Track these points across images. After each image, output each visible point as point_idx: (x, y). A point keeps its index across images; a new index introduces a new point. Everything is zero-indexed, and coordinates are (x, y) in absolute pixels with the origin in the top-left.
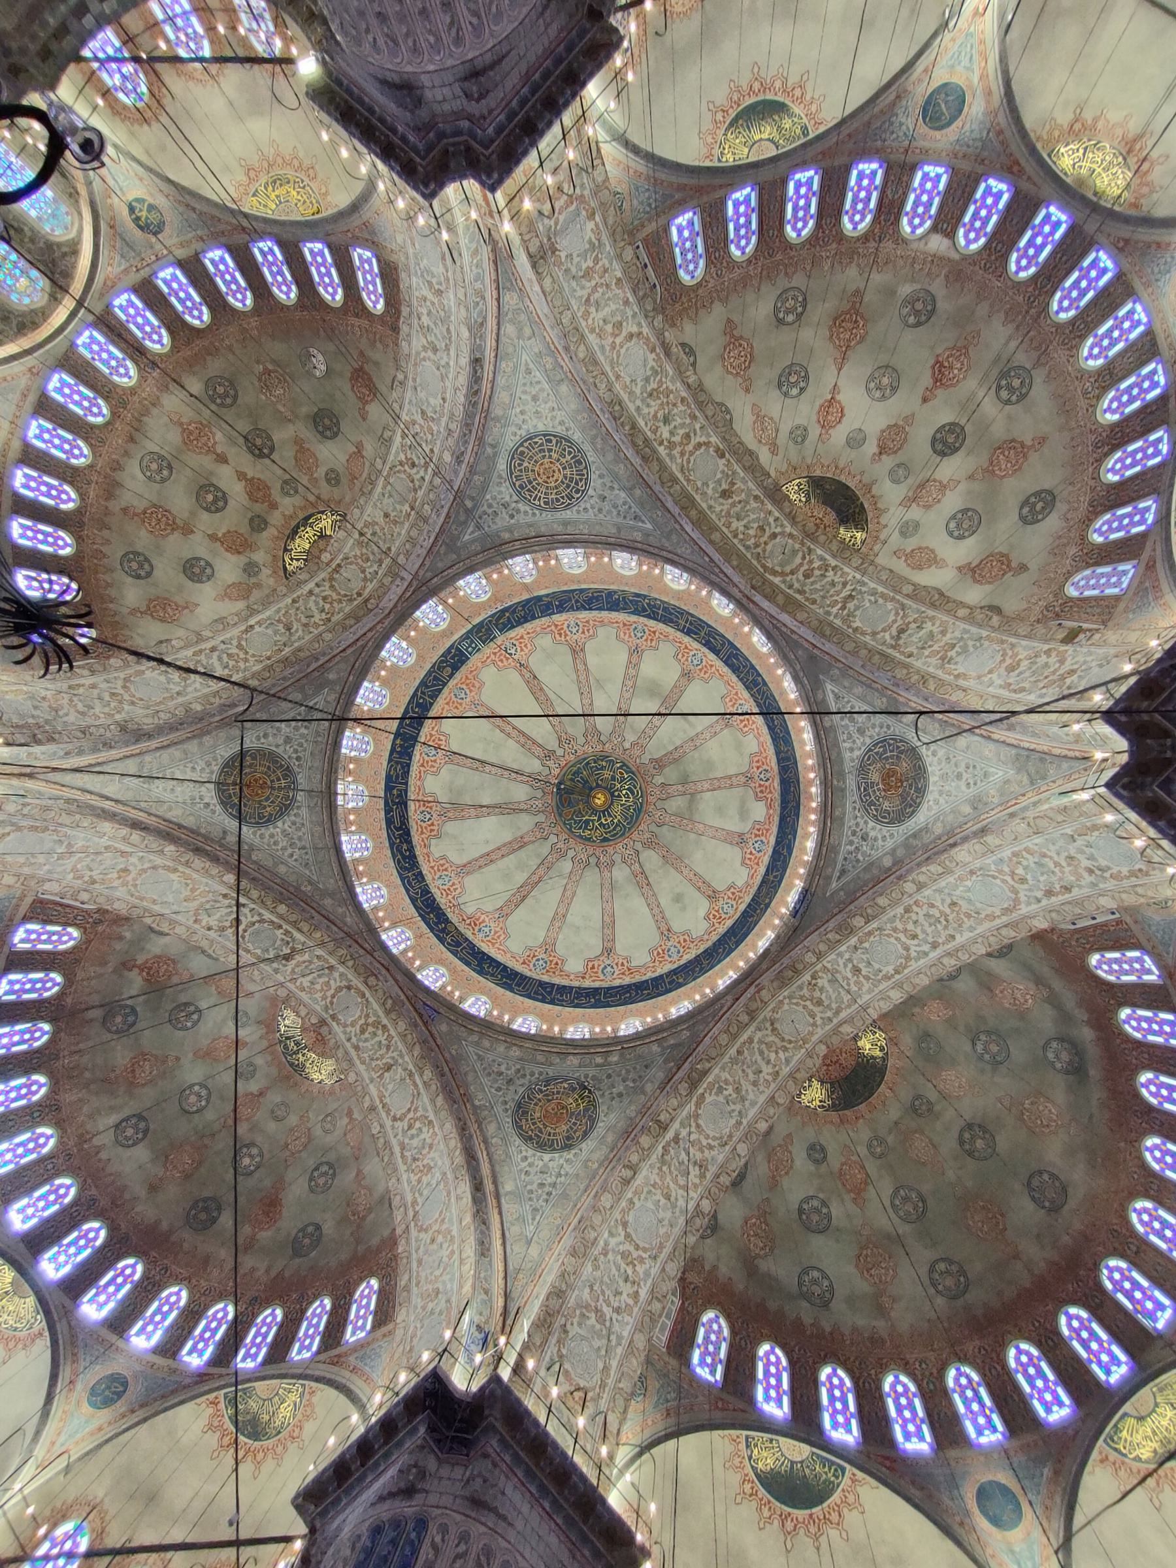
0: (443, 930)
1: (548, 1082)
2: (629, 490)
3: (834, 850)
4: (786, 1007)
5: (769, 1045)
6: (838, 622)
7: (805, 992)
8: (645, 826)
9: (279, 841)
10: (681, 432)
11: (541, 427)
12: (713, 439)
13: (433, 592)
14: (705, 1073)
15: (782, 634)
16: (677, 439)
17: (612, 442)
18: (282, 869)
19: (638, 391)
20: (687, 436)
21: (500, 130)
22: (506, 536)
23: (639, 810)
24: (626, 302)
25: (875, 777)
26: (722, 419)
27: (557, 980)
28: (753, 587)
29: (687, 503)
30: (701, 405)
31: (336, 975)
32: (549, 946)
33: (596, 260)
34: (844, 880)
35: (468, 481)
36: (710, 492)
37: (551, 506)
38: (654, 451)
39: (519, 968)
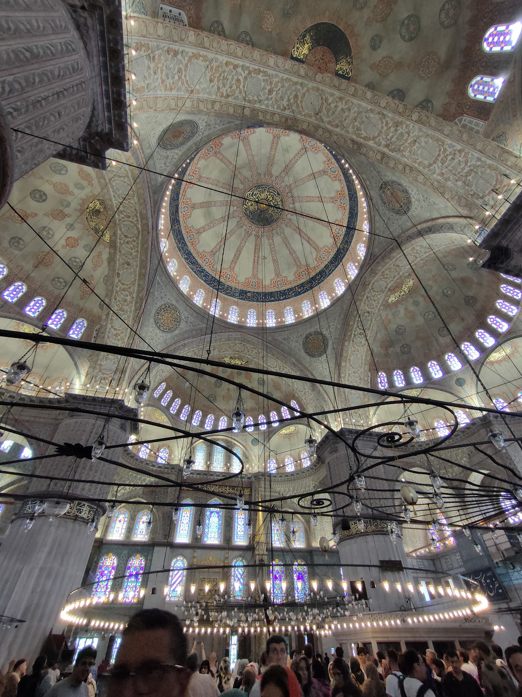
0: (343, 250)
1: (385, 203)
3: (223, 130)
4: (306, 111)
5: (328, 111)
6: (136, 198)
7: (294, 107)
8: (264, 180)
9: (330, 330)
11: (158, 331)
12: (117, 280)
13: (227, 323)
14: (353, 141)
15: (155, 208)
18: (339, 327)
20: (123, 290)
22: (195, 314)
23: (258, 187)
24: (108, 337)
25: (181, 139)
27: (346, 192)
28: (148, 233)
29: (142, 276)
30: (112, 292)
31: (369, 295)
32: (333, 200)
34: (232, 121)
35: (188, 338)
36: (132, 270)
37: (175, 309)
38: (137, 297)
39: (347, 211)
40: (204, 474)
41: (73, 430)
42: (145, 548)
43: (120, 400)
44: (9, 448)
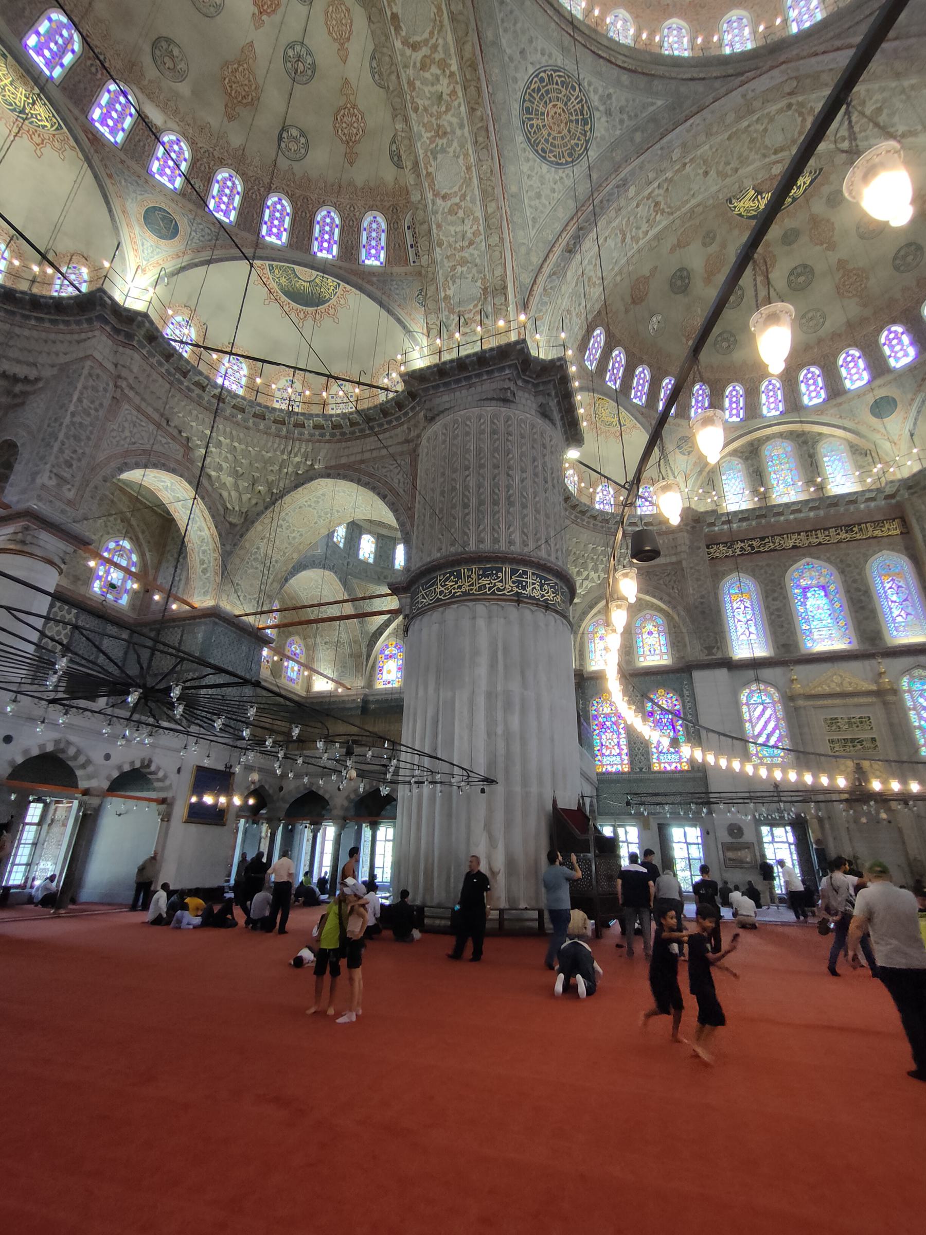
2: (495, 43)
10: (427, 75)
11: (545, 167)
12: (398, 44)
16: (435, 70)
17: (494, 110)
19: (455, 144)
21: (502, 369)
22: (625, 78)
24: (439, 226)
26: (383, 66)
30: (401, 94)
33: (453, 268)
35: (626, 160)
37: (570, 83)
38: (461, 68)
40: (758, 517)
41: (444, 442)
42: (671, 676)
43: (517, 343)
44: (372, 556)
